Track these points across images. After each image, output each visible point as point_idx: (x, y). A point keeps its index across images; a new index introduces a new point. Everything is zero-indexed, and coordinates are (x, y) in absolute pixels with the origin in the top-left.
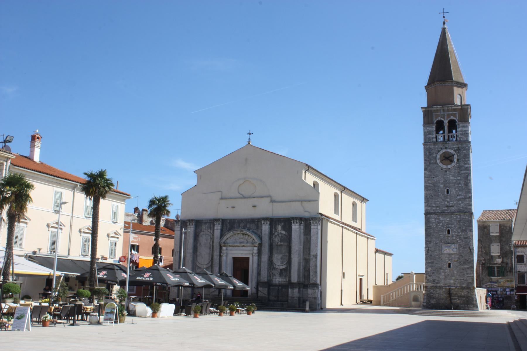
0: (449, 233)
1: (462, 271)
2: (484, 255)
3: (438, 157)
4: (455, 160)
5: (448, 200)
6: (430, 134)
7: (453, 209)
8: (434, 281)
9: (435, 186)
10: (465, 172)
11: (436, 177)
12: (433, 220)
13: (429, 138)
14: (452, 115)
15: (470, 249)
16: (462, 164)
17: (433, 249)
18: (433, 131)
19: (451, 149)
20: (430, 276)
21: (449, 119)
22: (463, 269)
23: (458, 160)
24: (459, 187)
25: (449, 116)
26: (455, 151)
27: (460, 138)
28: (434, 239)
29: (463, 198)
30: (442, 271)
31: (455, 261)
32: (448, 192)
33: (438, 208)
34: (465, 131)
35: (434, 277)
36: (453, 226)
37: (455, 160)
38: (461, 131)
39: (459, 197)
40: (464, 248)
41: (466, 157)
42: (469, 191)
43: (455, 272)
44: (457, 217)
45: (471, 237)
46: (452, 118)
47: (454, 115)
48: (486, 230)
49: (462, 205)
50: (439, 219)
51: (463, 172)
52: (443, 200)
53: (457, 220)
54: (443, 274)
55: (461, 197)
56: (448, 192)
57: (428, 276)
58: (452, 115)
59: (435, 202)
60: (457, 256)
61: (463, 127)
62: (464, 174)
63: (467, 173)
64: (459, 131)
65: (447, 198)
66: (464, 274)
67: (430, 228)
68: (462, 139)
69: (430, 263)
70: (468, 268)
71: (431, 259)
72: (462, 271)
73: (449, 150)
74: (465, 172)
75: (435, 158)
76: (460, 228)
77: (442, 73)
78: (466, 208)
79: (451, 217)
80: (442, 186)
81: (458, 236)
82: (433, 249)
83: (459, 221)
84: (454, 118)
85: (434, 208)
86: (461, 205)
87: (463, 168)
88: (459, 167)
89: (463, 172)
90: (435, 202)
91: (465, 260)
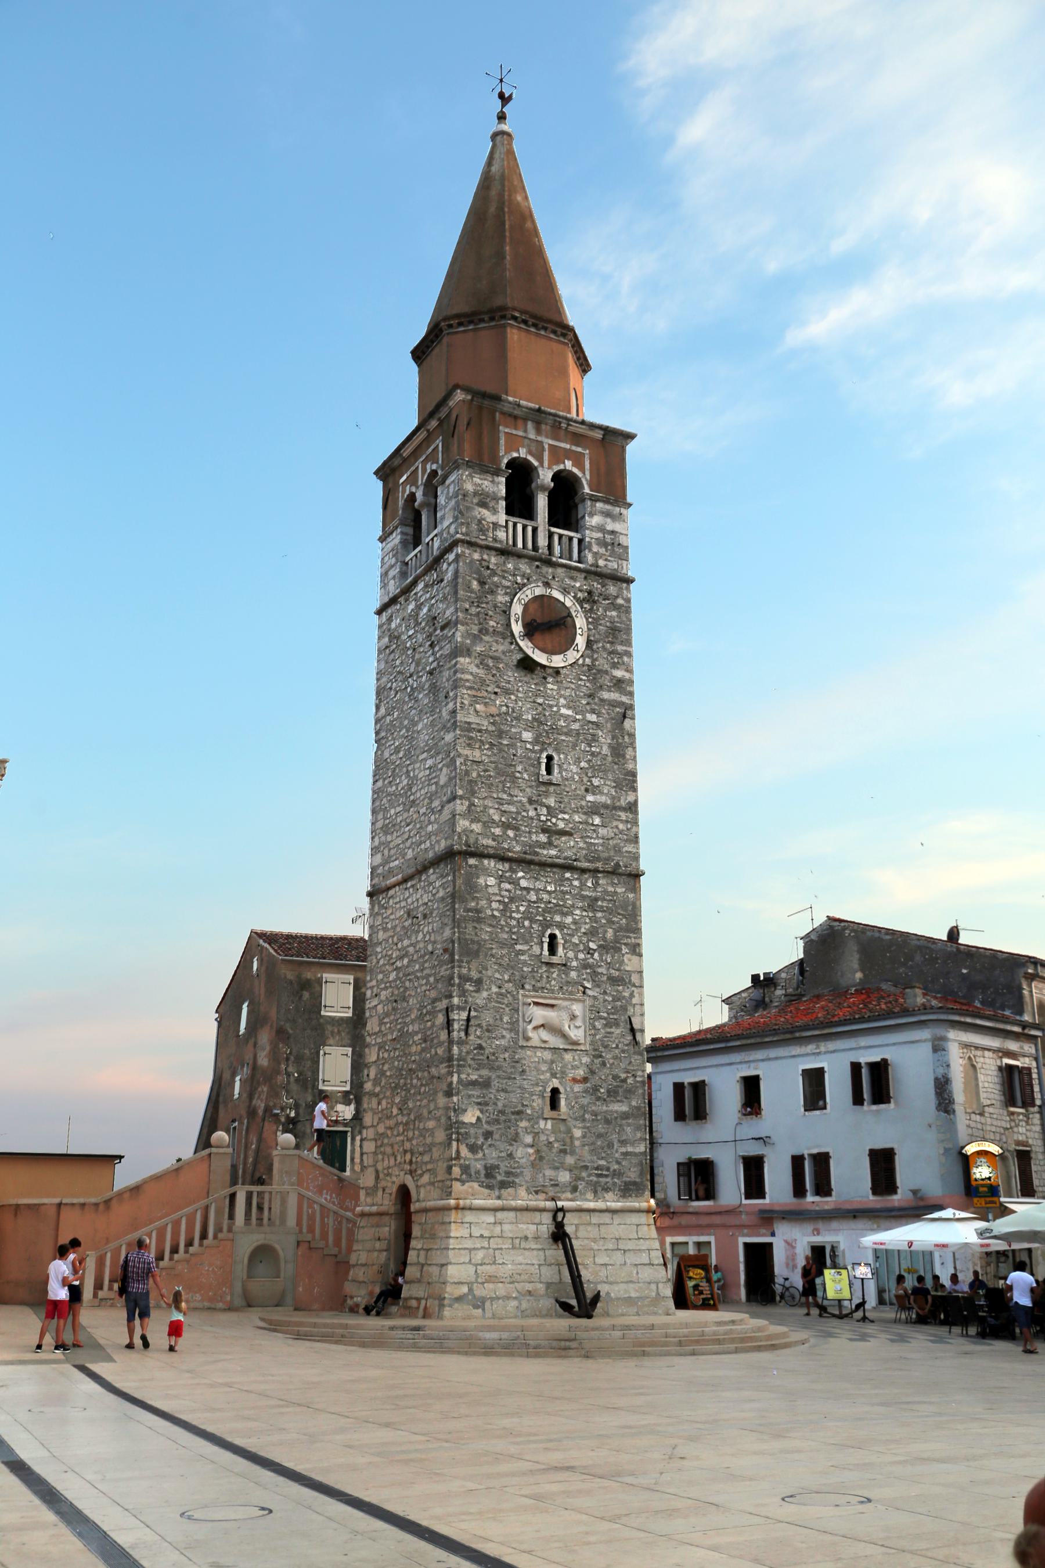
0: (552, 950)
1: (601, 1128)
2: (294, 1087)
3: (517, 609)
4: (581, 641)
5: (551, 801)
6: (483, 505)
7: (570, 847)
8: (490, 1172)
9: (501, 734)
10: (614, 696)
11: (507, 692)
12: (491, 881)
13: (480, 522)
14: (568, 454)
15: (633, 1031)
16: (602, 663)
17: (487, 1018)
18: (496, 499)
19: (565, 591)
20: (473, 1149)
21: (556, 468)
22: (607, 1122)
23: (589, 644)
24: (593, 754)
25: (557, 455)
26: (581, 602)
27: (596, 555)
28: (493, 971)
29: (605, 806)
30: (524, 1124)
31: (575, 1080)
32: (549, 770)
33: (511, 833)
34: (613, 532)
35: (492, 1156)
36: (569, 920)
37: (581, 641)
38: (601, 529)
39: (590, 798)
40: (608, 1025)
41: (616, 635)
42: (629, 781)
43: (578, 1133)
44: (583, 885)
45: (635, 978)
46: (569, 465)
47: (578, 462)
48: (306, 995)
49: (602, 831)
50: (515, 883)
51: (606, 695)
52: (531, 801)
53: (583, 898)
54: (529, 1139)
55: (603, 799)
56: (549, 770)
57: (464, 1152)
58: (568, 454)
59: (500, 802)
60: (585, 1060)
61: (608, 514)
62: (613, 704)
63: (621, 704)
64: (592, 529)
65: (547, 794)
66: (610, 1145)
67: (479, 920)
68: (601, 563)
69: (474, 1083)
70: (625, 1116)
71: (480, 1066)
72: (601, 1128)
73: (557, 594)
74: (614, 696)
75: (506, 612)
76: (592, 933)
77: (496, 301)
78: (618, 850)
79: (563, 879)
80: (527, 736)
81: (586, 966)
82: (487, 1018)
83: (592, 904)
84: (575, 470)
85: (498, 831)
86: (601, 832)
87: (606, 680)
88: (594, 672)
89: (606, 695)
90: (500, 802)
91: (615, 1077)
